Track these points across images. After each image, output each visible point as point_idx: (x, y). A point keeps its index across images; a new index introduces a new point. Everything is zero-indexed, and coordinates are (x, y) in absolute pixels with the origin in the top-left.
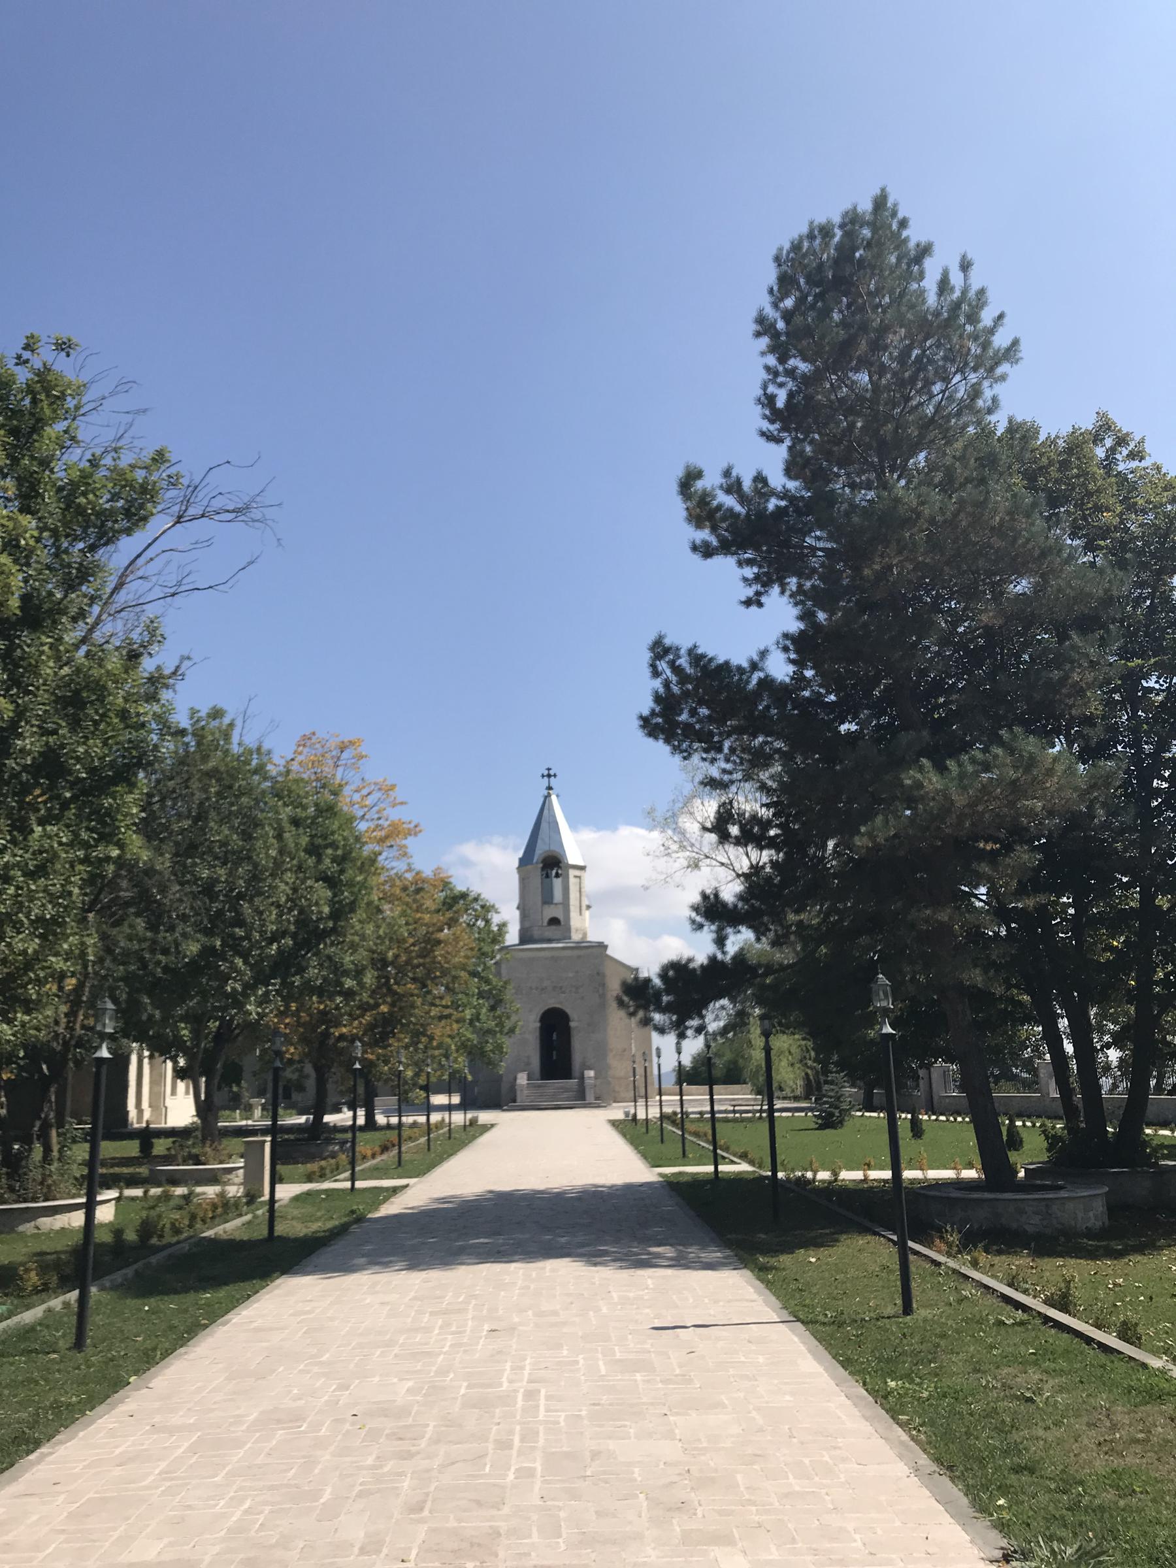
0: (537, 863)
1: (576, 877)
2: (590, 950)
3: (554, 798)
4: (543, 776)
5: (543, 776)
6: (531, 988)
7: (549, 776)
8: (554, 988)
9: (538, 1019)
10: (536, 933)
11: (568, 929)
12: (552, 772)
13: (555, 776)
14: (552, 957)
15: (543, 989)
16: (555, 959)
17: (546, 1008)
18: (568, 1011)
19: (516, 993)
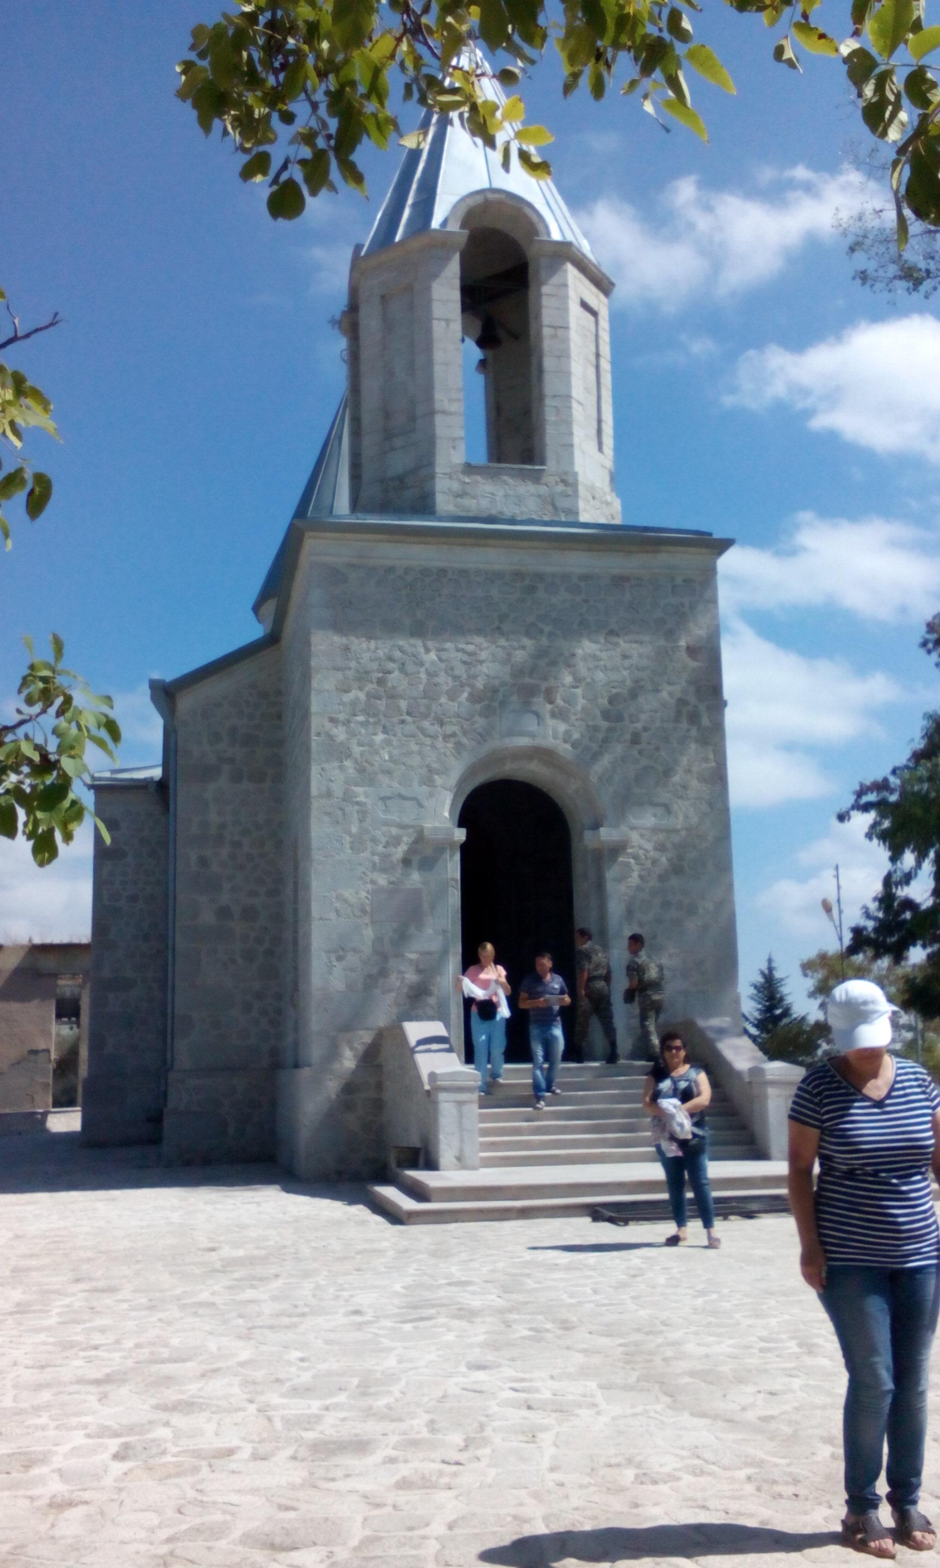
1: (584, 305)
2: (664, 558)
14: (518, 575)
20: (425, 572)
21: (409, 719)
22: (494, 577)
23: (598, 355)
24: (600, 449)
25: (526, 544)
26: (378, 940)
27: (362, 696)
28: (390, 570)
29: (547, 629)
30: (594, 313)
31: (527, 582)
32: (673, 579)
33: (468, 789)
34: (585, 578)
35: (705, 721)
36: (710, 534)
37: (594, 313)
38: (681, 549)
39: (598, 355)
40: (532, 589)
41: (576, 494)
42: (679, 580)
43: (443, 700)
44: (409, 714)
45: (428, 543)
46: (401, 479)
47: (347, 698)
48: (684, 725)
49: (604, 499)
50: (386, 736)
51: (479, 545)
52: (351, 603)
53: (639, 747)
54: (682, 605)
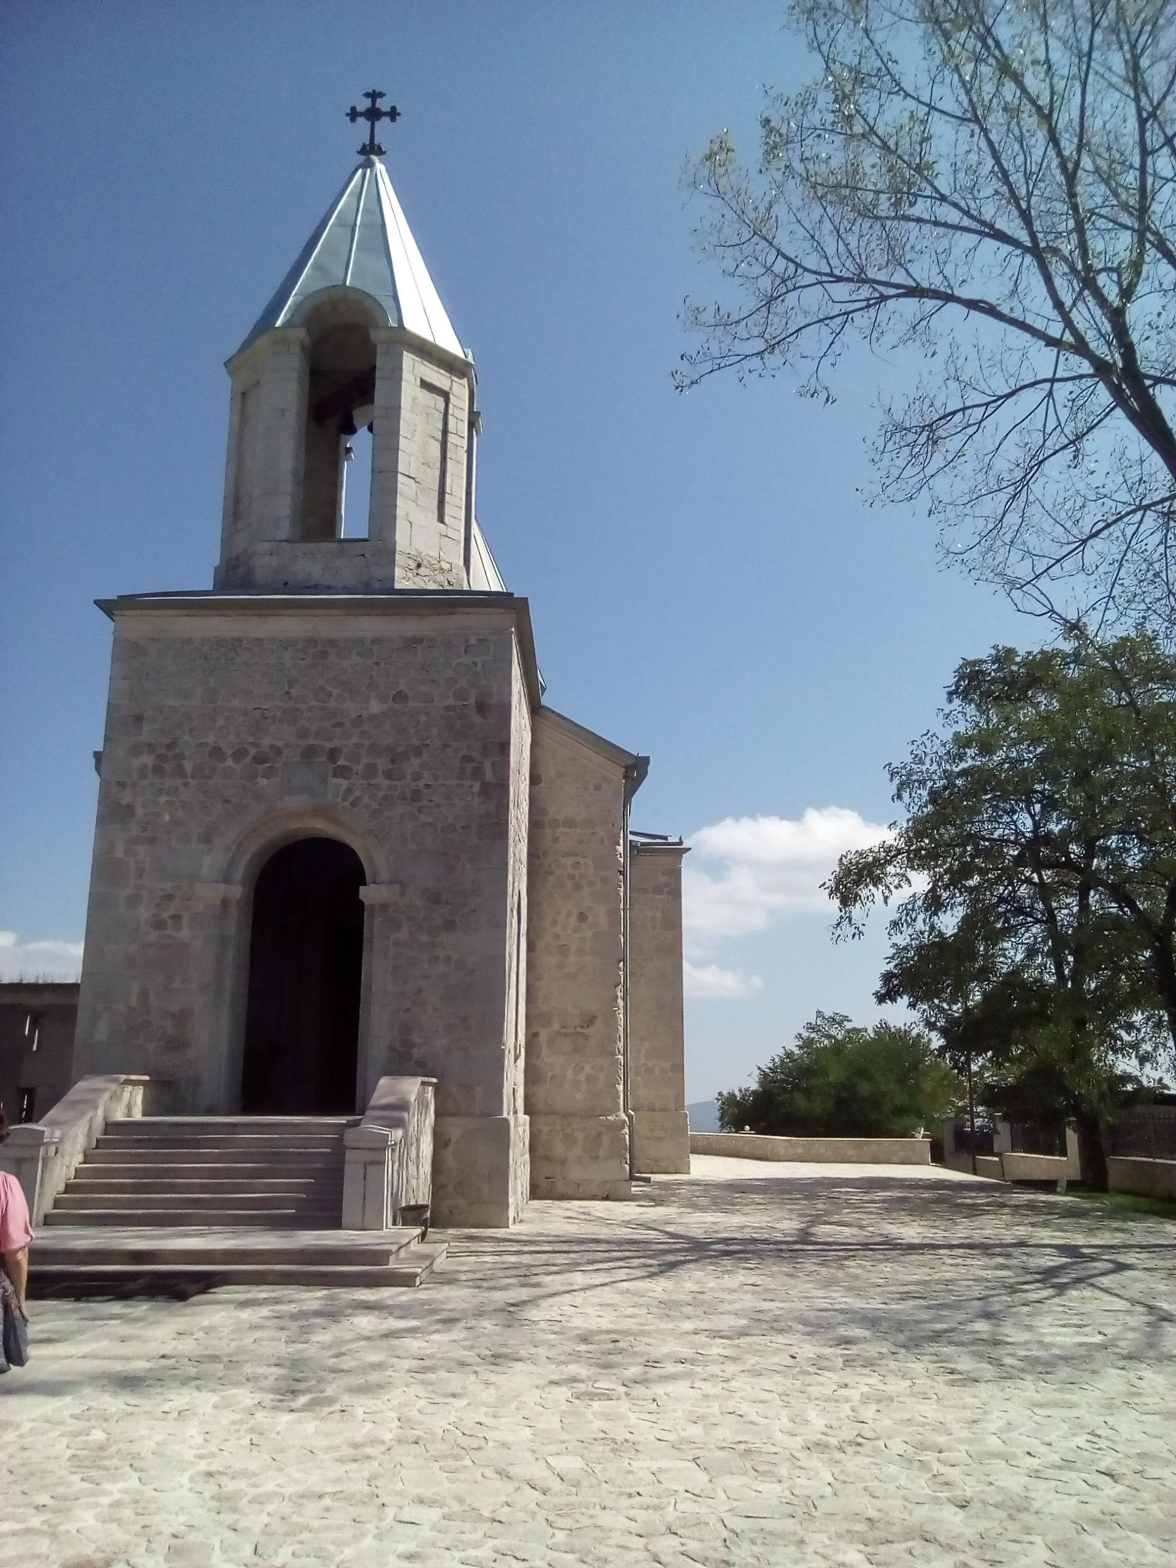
0: (288, 324)
1: (426, 385)
3: (380, 167)
4: (353, 114)
5: (353, 114)
6: (217, 752)
7: (373, 115)
8: (309, 753)
9: (239, 873)
10: (264, 564)
11: (387, 554)
12: (383, 105)
13: (393, 114)
14: (312, 641)
15: (260, 759)
16: (320, 648)
17: (275, 832)
18: (356, 844)
19: (158, 770)
20: (220, 643)
21: (191, 781)
22: (287, 644)
23: (445, 432)
24: (441, 519)
25: (320, 612)
26: (144, 993)
27: (147, 760)
28: (189, 641)
29: (335, 692)
30: (446, 395)
31: (320, 648)
32: (467, 640)
33: (253, 847)
34: (376, 641)
35: (489, 776)
36: (513, 594)
37: (446, 395)
38: (475, 610)
39: (445, 432)
40: (324, 654)
41: (392, 563)
42: (473, 641)
43: (229, 762)
44: (193, 777)
45: (227, 616)
46: (237, 558)
47: (137, 762)
48: (467, 783)
49: (437, 567)
50: (168, 798)
51: (275, 615)
52: (147, 674)
53: (416, 804)
54: (475, 664)
